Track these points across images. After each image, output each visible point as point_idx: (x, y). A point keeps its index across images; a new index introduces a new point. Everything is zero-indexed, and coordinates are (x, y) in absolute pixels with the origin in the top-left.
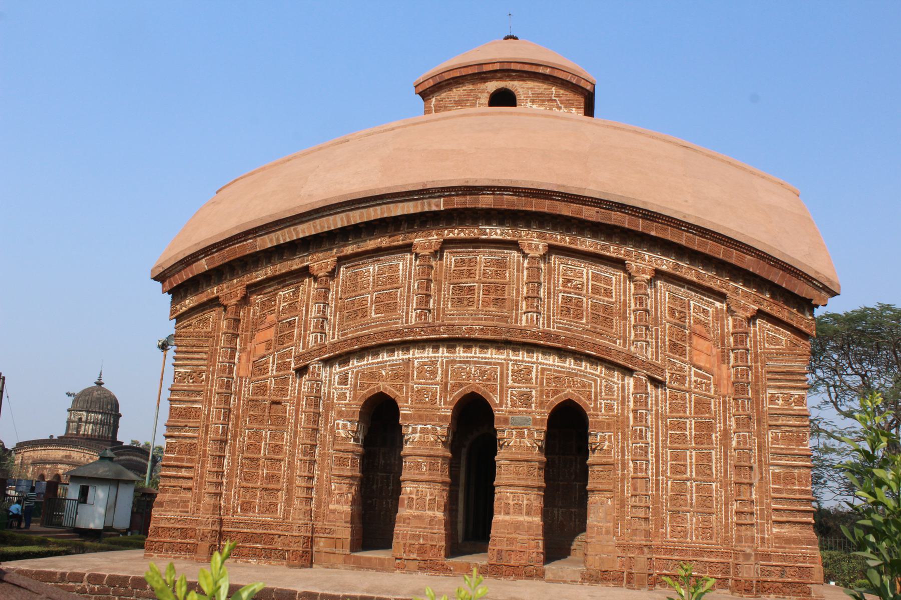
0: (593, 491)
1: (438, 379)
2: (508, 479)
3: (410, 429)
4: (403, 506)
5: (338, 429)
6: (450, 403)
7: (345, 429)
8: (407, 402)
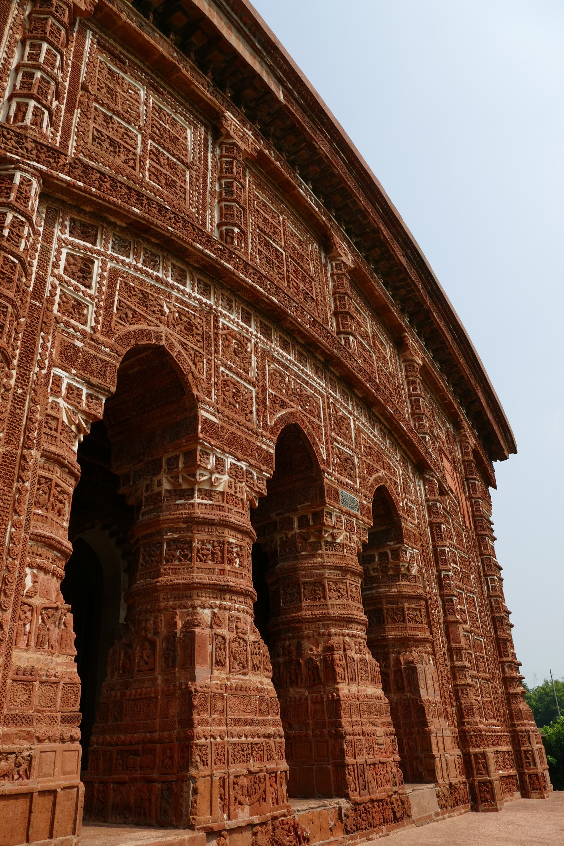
1: (253, 374)
3: (213, 459)
5: (57, 393)
7: (69, 402)
8: (209, 396)
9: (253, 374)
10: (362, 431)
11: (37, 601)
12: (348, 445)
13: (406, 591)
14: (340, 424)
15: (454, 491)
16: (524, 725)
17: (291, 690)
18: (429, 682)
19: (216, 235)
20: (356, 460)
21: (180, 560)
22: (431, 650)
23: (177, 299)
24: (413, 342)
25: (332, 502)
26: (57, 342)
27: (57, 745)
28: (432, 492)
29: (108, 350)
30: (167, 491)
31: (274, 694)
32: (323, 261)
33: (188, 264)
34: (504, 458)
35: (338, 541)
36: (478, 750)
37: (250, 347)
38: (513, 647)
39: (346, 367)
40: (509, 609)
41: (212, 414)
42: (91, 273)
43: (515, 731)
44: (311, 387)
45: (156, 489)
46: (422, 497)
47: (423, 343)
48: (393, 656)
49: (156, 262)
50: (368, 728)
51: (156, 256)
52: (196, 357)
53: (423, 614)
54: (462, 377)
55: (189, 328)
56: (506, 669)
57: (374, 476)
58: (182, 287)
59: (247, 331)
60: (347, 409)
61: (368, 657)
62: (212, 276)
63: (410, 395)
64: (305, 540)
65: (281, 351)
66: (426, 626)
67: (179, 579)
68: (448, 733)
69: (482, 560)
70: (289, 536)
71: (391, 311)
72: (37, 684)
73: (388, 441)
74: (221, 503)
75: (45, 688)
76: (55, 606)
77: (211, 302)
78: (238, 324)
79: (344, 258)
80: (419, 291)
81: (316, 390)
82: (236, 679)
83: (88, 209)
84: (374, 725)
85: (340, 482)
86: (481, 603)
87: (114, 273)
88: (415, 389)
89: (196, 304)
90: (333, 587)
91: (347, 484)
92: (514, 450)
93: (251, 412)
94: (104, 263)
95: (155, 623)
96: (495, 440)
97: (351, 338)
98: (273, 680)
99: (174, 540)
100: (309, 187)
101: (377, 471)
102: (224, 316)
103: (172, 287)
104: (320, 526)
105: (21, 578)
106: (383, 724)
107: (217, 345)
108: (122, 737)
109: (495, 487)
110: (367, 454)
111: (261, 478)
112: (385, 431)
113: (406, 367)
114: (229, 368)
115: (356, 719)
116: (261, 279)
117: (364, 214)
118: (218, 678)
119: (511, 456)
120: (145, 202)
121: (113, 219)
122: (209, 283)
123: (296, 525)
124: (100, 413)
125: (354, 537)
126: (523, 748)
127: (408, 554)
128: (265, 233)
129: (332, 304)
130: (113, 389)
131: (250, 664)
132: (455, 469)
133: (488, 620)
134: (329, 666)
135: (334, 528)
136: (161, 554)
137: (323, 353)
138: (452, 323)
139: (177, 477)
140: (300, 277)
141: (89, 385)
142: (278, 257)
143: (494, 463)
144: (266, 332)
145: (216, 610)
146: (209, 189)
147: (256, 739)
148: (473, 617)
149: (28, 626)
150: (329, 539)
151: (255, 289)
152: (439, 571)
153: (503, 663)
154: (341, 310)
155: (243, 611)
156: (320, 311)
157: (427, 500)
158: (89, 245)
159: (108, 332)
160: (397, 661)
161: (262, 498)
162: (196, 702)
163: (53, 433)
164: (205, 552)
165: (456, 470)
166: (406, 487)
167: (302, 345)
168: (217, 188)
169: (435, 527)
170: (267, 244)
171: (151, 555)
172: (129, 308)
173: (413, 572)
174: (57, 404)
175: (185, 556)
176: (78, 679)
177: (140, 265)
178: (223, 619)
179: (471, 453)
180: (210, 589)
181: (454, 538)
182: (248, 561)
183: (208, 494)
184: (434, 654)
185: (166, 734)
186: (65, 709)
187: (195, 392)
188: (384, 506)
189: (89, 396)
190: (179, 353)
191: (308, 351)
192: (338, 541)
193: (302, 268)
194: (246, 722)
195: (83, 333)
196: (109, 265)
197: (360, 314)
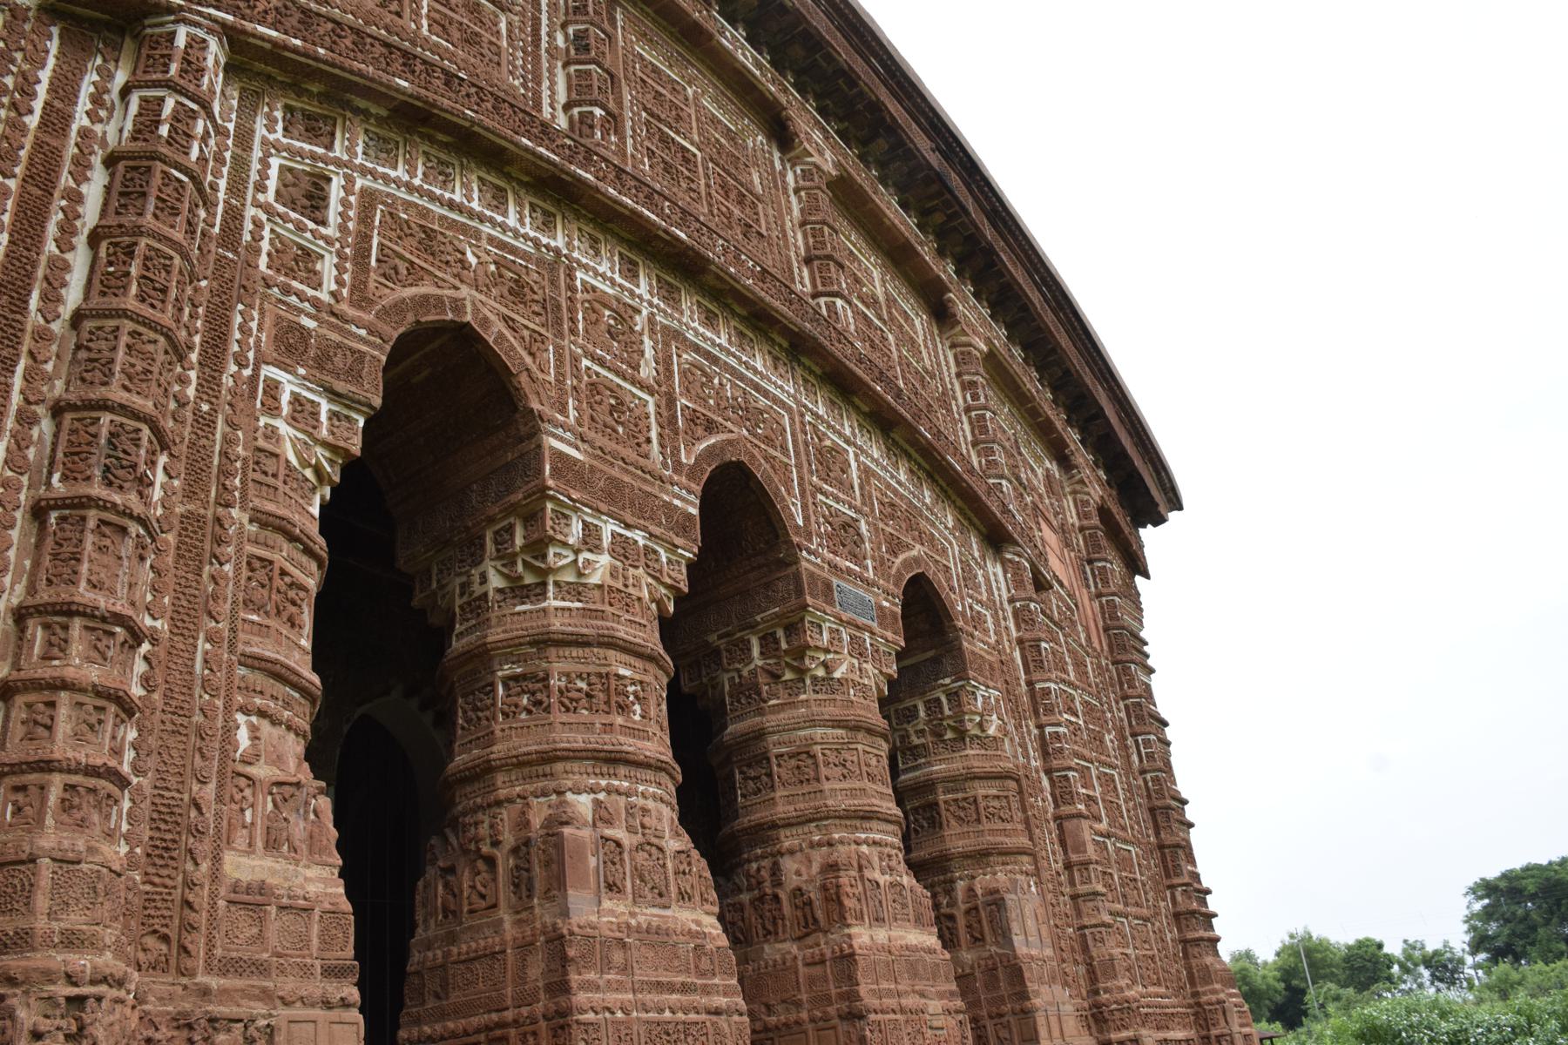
0: (981, 857)
1: (647, 371)
2: (852, 792)
3: (576, 528)
4: (582, 884)
6: (692, 473)
8: (563, 410)
9: (647, 371)
10: (875, 475)
11: (260, 771)
12: (846, 498)
13: (979, 766)
14: (829, 462)
15: (1066, 583)
16: (1214, 992)
17: (766, 947)
18: (1030, 923)
19: (562, 122)
20: (864, 527)
21: (529, 712)
22: (1031, 868)
23: (491, 240)
24: (967, 306)
25: (820, 603)
26: (268, 322)
27: (317, 1013)
28: (1019, 583)
29: (363, 332)
30: (499, 591)
31: (724, 941)
32: (778, 166)
33: (509, 177)
34: (1159, 520)
35: (837, 675)
36: (1124, 1034)
37: (640, 322)
38: (1192, 862)
39: (832, 355)
40: (1184, 795)
41: (569, 444)
42: (325, 198)
43: (1199, 1004)
44: (766, 394)
45: (477, 589)
46: (1003, 592)
47: (986, 312)
48: (961, 885)
49: (447, 175)
50: (910, 1001)
51: (447, 164)
52: (534, 344)
53: (1015, 805)
54: (1067, 372)
55: (517, 291)
56: (1179, 898)
57: (902, 557)
58: (499, 219)
59: (632, 293)
60: (840, 434)
61: (907, 880)
62: (557, 193)
63: (968, 410)
64: (776, 677)
65: (701, 330)
66: (1020, 827)
67: (528, 745)
68: (1068, 1008)
69: (1126, 707)
70: (745, 673)
71: (918, 254)
72: (273, 910)
73: (927, 493)
74: (599, 606)
75: (287, 918)
76: (294, 780)
77: (559, 242)
78: (613, 283)
79: (816, 159)
80: (967, 213)
81: (775, 400)
82: (648, 915)
83: (315, 88)
84: (922, 995)
85: (834, 567)
86: (1129, 784)
87: (369, 200)
88: (975, 397)
89: (529, 248)
90: (832, 758)
91: (849, 571)
92: (1177, 505)
93: (649, 441)
94: (350, 180)
95: (492, 826)
96: (1138, 487)
97: (839, 302)
98: (721, 918)
99: (516, 678)
100: (740, 35)
101: (909, 547)
102: (586, 268)
103: (481, 218)
104: (800, 652)
105: (229, 730)
106: (941, 995)
107: (573, 320)
108: (451, 1025)
109: (1147, 576)
110: (884, 517)
111: (675, 559)
112: (920, 474)
113: (955, 357)
114: (601, 362)
115: (885, 985)
116: (651, 197)
117: (851, 78)
118: (612, 912)
119: (1173, 516)
120: (419, 67)
121: (361, 103)
122: (552, 209)
123: (756, 651)
124: (356, 446)
125: (868, 667)
126: (1214, 1032)
127: (980, 699)
128: (659, 120)
129: (800, 242)
130: (377, 402)
131: (673, 889)
132: (1067, 544)
133: (1143, 814)
134: (834, 898)
135: (827, 651)
136: (494, 705)
137: (786, 331)
138: (1038, 272)
139: (514, 563)
140: (733, 195)
141: (333, 395)
142: (686, 160)
143: (1142, 531)
144: (669, 294)
145: (602, 796)
146: (544, 45)
147: (693, 1016)
148: (1113, 808)
149: (248, 813)
150: (821, 673)
151: (641, 215)
152: (1040, 727)
153: (1172, 887)
154: (817, 253)
155: (656, 802)
156: (777, 257)
157: (1011, 601)
158: (321, 151)
159: (361, 298)
160: (970, 890)
161: (680, 599)
162: (571, 953)
163: (270, 480)
164: (574, 694)
165: (1067, 545)
166: (968, 578)
167: (743, 319)
168: (560, 40)
169: (1029, 646)
170: (665, 141)
171: (475, 709)
172: (401, 257)
173: (992, 731)
174: (274, 430)
175: (538, 703)
176: (347, 906)
177: (417, 182)
178: (611, 808)
179: (1095, 513)
180: (587, 758)
181: (1070, 668)
182: (660, 710)
183: (576, 591)
184: (1038, 876)
185: (525, 1011)
186: (327, 955)
187: (535, 405)
188: (924, 612)
189: (333, 415)
190: (501, 335)
191: (755, 329)
192: (837, 675)
193: (736, 180)
194: (671, 988)
195: (316, 303)
196: (360, 183)
197: (860, 262)
